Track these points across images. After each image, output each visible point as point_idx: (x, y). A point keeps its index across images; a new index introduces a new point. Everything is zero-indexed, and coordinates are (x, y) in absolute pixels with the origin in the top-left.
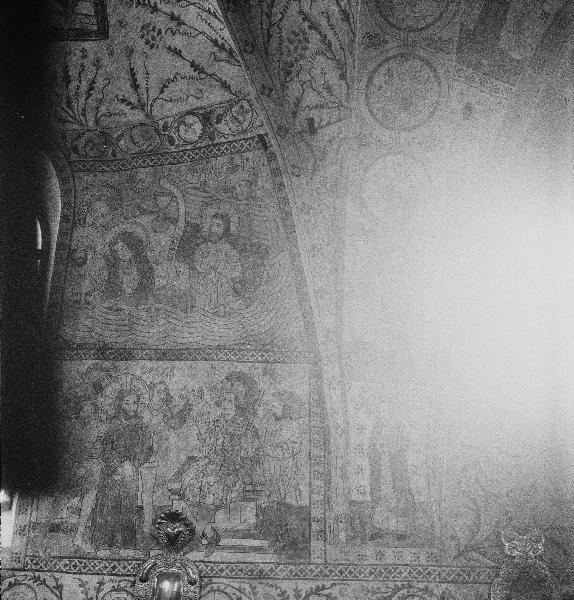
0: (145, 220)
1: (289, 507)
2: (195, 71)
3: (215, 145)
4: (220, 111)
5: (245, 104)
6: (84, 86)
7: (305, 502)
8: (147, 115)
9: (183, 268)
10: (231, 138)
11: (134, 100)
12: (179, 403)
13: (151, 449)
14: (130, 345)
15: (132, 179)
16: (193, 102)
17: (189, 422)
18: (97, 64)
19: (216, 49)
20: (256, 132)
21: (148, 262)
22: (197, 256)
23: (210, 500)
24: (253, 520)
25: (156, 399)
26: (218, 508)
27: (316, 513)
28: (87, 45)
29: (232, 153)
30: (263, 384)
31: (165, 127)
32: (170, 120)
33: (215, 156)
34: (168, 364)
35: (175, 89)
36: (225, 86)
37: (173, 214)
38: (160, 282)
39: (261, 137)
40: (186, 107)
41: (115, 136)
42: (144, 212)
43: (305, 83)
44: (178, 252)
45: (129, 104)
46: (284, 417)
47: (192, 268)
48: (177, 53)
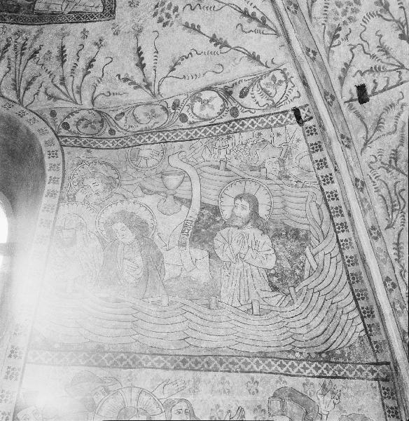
0: (148, 200)
2: (216, 45)
4: (242, 85)
5: (279, 76)
6: (82, 64)
8: (154, 95)
9: (200, 254)
10: (258, 113)
11: (138, 79)
14: (135, 348)
16: (211, 79)
18: (99, 44)
19: (246, 19)
22: (218, 241)
28: (88, 26)
29: (259, 128)
31: (175, 106)
32: (182, 98)
34: (190, 374)
36: (254, 58)
37: (182, 193)
38: (170, 270)
39: (296, 111)
40: (201, 83)
41: (113, 115)
42: (149, 192)
43: (355, 47)
44: (192, 239)
45: (134, 83)
48: (194, 29)
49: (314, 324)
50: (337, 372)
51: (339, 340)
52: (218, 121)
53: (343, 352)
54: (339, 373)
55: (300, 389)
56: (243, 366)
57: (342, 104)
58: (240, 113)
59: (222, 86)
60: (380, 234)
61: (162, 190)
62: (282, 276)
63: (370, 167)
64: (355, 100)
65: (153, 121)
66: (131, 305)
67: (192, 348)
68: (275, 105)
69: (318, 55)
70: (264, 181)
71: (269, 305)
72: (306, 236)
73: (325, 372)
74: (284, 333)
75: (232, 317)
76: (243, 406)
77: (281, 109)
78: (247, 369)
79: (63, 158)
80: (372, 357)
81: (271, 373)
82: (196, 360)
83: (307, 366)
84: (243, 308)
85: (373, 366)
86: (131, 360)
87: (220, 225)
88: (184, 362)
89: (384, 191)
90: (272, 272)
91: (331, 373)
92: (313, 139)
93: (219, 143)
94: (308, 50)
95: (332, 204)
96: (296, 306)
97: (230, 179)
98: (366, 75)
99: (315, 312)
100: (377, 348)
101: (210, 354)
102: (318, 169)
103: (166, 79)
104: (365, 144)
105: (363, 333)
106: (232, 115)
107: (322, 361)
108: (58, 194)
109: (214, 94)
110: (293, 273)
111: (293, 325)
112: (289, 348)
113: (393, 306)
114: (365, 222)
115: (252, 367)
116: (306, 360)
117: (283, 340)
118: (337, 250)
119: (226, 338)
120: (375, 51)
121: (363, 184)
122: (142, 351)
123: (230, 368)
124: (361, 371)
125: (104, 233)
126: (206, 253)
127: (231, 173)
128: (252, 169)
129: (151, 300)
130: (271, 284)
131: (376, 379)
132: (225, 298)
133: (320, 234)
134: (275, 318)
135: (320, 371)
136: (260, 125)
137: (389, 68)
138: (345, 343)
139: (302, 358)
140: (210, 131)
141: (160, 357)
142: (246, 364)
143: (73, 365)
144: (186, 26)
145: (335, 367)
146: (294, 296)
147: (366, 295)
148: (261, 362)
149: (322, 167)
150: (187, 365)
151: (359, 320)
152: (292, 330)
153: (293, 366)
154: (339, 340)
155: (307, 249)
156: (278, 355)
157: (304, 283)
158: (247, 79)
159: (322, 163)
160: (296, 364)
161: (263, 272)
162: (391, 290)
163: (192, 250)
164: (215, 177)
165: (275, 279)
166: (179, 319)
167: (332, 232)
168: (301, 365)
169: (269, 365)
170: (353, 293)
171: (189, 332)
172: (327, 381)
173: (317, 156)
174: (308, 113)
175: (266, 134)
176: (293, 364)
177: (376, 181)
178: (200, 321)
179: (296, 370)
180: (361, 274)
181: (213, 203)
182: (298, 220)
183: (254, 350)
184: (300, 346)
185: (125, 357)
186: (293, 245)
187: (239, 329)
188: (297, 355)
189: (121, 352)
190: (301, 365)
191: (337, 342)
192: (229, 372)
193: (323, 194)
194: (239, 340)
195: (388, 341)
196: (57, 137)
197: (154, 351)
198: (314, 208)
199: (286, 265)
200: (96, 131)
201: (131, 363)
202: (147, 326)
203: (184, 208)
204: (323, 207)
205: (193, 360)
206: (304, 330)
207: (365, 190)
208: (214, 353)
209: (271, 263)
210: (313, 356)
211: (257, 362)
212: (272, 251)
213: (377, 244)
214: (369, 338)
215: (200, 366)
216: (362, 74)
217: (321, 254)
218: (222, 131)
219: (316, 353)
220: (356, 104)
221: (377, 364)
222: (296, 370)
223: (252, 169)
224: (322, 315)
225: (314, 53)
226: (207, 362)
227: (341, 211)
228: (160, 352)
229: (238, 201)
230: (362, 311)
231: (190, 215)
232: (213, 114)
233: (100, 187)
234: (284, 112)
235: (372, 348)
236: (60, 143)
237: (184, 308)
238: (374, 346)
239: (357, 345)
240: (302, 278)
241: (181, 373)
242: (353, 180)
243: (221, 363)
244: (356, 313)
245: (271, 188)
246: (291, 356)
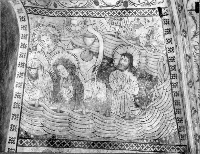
0: (77, 52)
3: (126, 9)
9: (101, 85)
10: (139, 7)
14: (70, 137)
15: (69, 23)
20: (156, 6)
21: (79, 80)
22: (111, 78)
29: (138, 15)
33: (127, 16)
37: (94, 49)
38: (87, 94)
39: (160, 9)
44: (98, 76)
49: (155, 125)
50: (162, 149)
51: (165, 133)
52: (116, 8)
53: (166, 140)
54: (163, 150)
56: (120, 147)
57: (186, 11)
58: (129, 5)
60: (193, 84)
61: (84, 45)
62: (141, 99)
63: (194, 48)
64: (194, 10)
66: (68, 114)
67: (97, 137)
70: (137, 47)
71: (134, 115)
72: (155, 79)
73: (157, 149)
74: (140, 130)
75: (116, 120)
77: (152, 7)
78: (122, 149)
79: (29, 22)
80: (179, 142)
81: (133, 150)
82: (99, 144)
83: (149, 146)
84: (121, 116)
85: (178, 147)
86: (69, 143)
87: (112, 69)
88: (93, 144)
90: (137, 97)
91: (159, 149)
92: (166, 27)
93: (116, 22)
95: (171, 64)
96: (146, 115)
97: (120, 43)
99: (155, 119)
100: (182, 138)
101: (106, 140)
102: (167, 43)
105: (177, 130)
106: (124, 5)
107: (156, 144)
108: (27, 46)
111: (143, 125)
112: (141, 138)
113: (193, 123)
114: (187, 79)
115: (124, 147)
116: (149, 143)
117: (139, 133)
118: (170, 87)
119: (113, 132)
121: (190, 57)
122: (74, 139)
123: (114, 148)
124: (173, 148)
125: (53, 71)
126: (105, 85)
127: (121, 40)
128: (132, 39)
129: (78, 111)
130: (136, 103)
133: (163, 79)
134: (136, 122)
135: (155, 149)
136: (139, 14)
138: (167, 135)
139: (147, 142)
140: (111, 13)
141: (82, 142)
142: (122, 146)
143: (41, 146)
145: (162, 147)
146: (146, 110)
147: (180, 111)
148: (128, 145)
149: (169, 43)
150: (95, 146)
151: (176, 124)
152: (143, 128)
153: (143, 147)
154: (165, 133)
155: (155, 86)
156: (136, 141)
157: (152, 103)
159: (169, 41)
160: (144, 146)
161: (132, 97)
162: (194, 114)
163: (98, 83)
164: (112, 42)
165: (138, 101)
166: (91, 122)
167: (169, 78)
168: (147, 146)
169: (132, 146)
170: (174, 110)
171: (96, 129)
173: (168, 36)
174: (166, 12)
175: (142, 20)
176: (143, 145)
177: (196, 55)
178: (101, 123)
179: (144, 148)
180: (180, 100)
181: (111, 57)
182: (153, 70)
183: (126, 139)
184: (146, 136)
185: (65, 142)
186: (148, 83)
187: (119, 127)
188: (145, 141)
189: (64, 140)
190: (147, 146)
191: (164, 134)
192: (114, 150)
193: (168, 57)
194: (119, 133)
195: (187, 135)
196: (24, 7)
197: (80, 139)
198: (162, 65)
199: (144, 93)
200: (46, 4)
201: (68, 145)
202: (76, 125)
203: (94, 58)
204: (167, 65)
205: (98, 144)
206: (150, 128)
207: (190, 61)
208: (108, 140)
209: (136, 92)
210: (152, 141)
211: (127, 145)
212: (137, 86)
213: (191, 90)
214: (179, 133)
215: (100, 146)
217: (162, 90)
218: (118, 14)
219: (154, 140)
220: (194, 13)
221: (181, 146)
222: (144, 148)
223: (132, 39)
224: (158, 121)
226: (104, 145)
227: (175, 68)
228: (82, 140)
229: (123, 57)
230: (177, 119)
231: (97, 62)
233: (50, 42)
234: (154, 9)
235: (180, 137)
236: (26, 11)
237: (94, 116)
238: (181, 137)
239: (173, 136)
240: (151, 101)
242: (185, 55)
243: (110, 145)
244: (174, 121)
245: (141, 51)
246: (142, 141)
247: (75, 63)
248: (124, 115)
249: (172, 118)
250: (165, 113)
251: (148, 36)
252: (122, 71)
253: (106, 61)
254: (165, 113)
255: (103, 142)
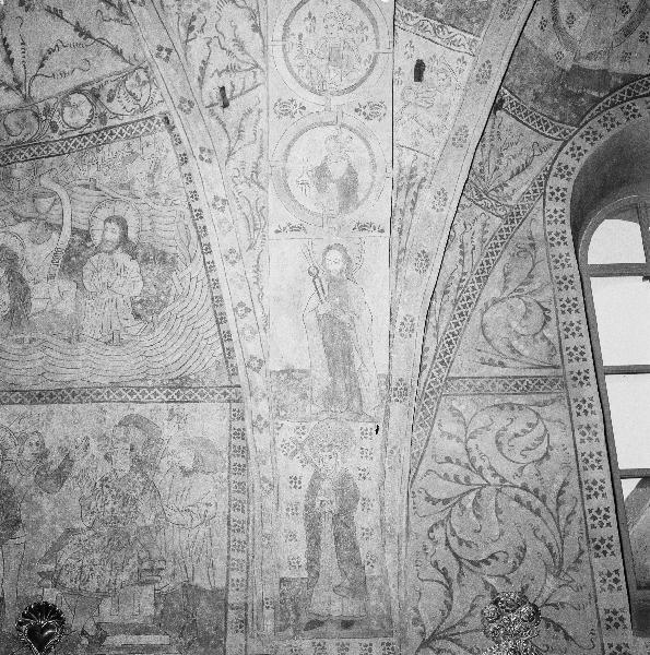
0: (22, 228)
1: (199, 590)
3: (106, 129)
5: (143, 77)
7: (220, 584)
9: (66, 285)
10: (127, 119)
12: (56, 458)
13: (19, 521)
16: (78, 78)
17: (69, 483)
23: (93, 584)
24: (149, 610)
25: (27, 452)
26: (105, 595)
27: (234, 598)
30: (169, 431)
31: (47, 110)
34: (44, 408)
35: (54, 63)
37: (54, 217)
40: (68, 84)
42: (19, 219)
46: (195, 470)
47: (80, 286)
52: (87, 130)
55: (148, 415)
59: (89, 88)
60: (240, 257)
65: (24, 132)
68: (143, 110)
69: (174, 54)
76: (89, 436)
77: (148, 114)
89: (246, 209)
90: (138, 299)
91: (181, 398)
94: (160, 49)
98: (223, 75)
103: (37, 78)
104: (229, 156)
105: (222, 357)
109: (82, 97)
110: (158, 300)
120: (230, 46)
124: (213, 394)
127: (101, 193)
128: (122, 186)
131: (229, 401)
132: (87, 332)
137: (244, 67)
144: (48, 10)
153: (144, 394)
158: (113, 78)
165: (139, 306)
172: (175, 406)
179: (146, 397)
181: (86, 228)
183: (106, 382)
186: (158, 269)
203: (55, 236)
204: (191, 227)
212: (140, 278)
216: (220, 74)
220: (218, 109)
222: (146, 397)
223: (122, 186)
225: (169, 51)
232: (83, 122)
234: (152, 118)
240: (165, 305)
241: (37, 407)
247: (18, 249)
248: (110, 338)
249: (212, 333)
250: (197, 325)
251: (151, 176)
252: (111, 253)
253: (77, 237)
254: (197, 325)
255: (60, 390)
